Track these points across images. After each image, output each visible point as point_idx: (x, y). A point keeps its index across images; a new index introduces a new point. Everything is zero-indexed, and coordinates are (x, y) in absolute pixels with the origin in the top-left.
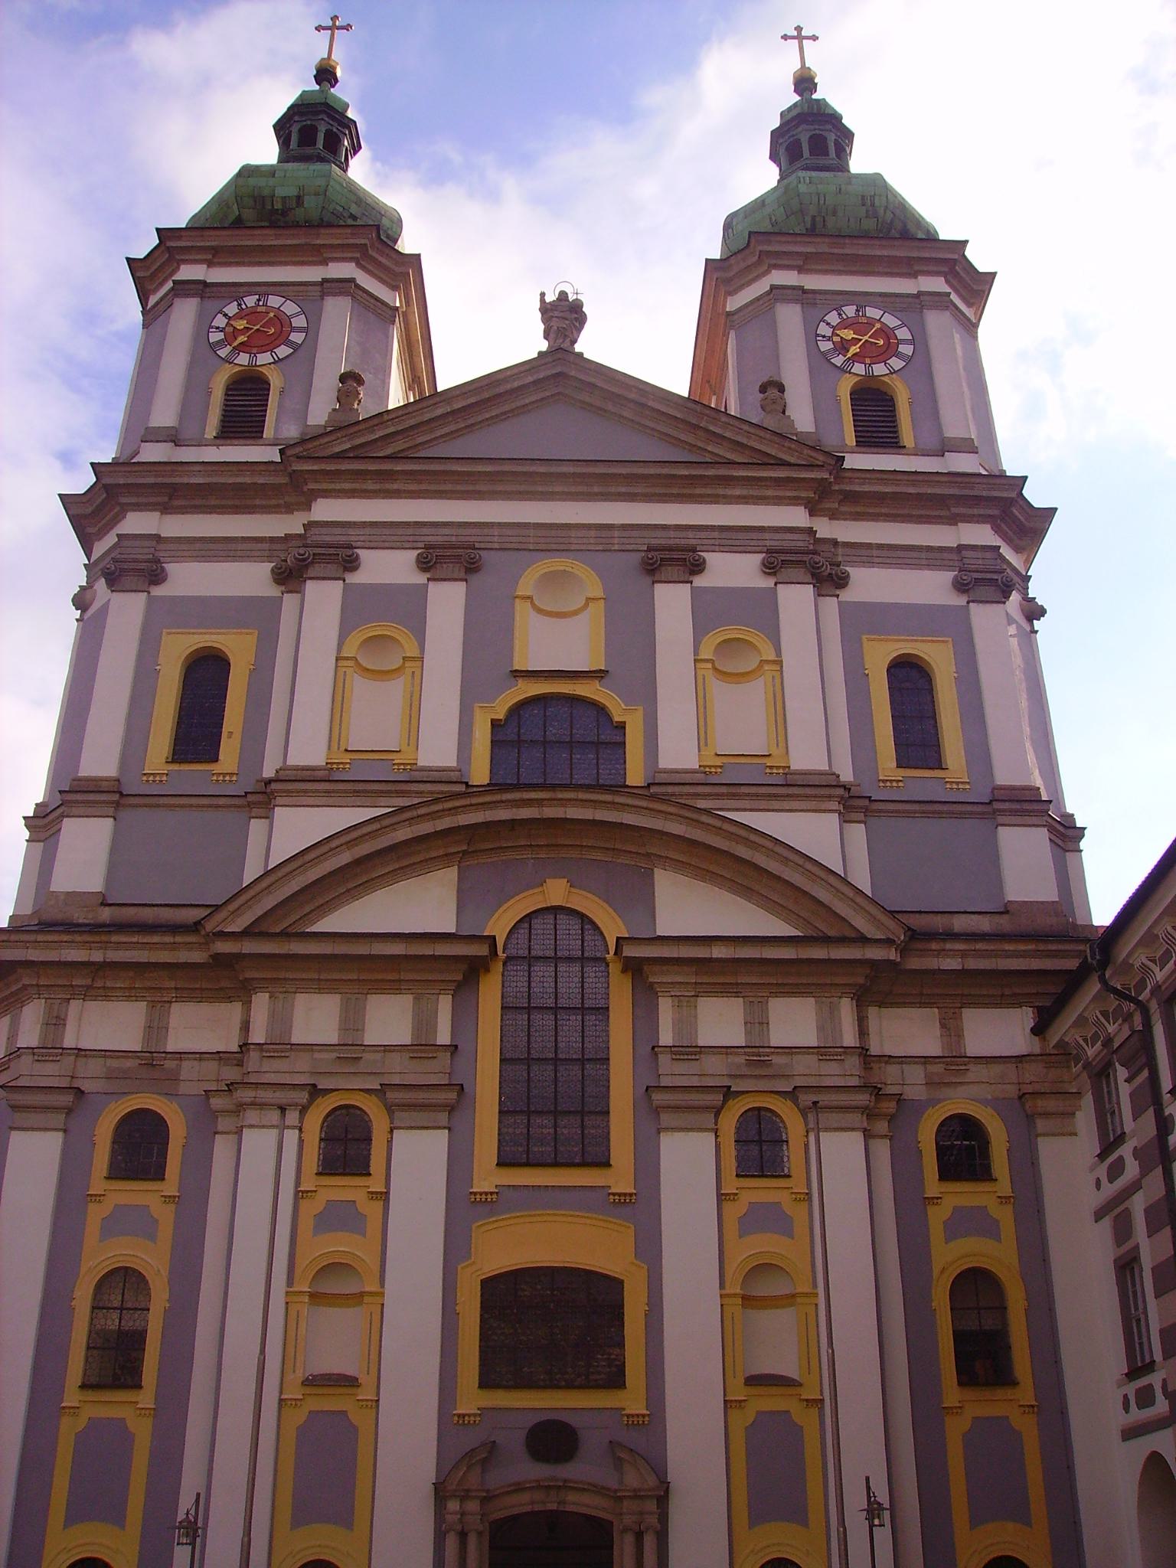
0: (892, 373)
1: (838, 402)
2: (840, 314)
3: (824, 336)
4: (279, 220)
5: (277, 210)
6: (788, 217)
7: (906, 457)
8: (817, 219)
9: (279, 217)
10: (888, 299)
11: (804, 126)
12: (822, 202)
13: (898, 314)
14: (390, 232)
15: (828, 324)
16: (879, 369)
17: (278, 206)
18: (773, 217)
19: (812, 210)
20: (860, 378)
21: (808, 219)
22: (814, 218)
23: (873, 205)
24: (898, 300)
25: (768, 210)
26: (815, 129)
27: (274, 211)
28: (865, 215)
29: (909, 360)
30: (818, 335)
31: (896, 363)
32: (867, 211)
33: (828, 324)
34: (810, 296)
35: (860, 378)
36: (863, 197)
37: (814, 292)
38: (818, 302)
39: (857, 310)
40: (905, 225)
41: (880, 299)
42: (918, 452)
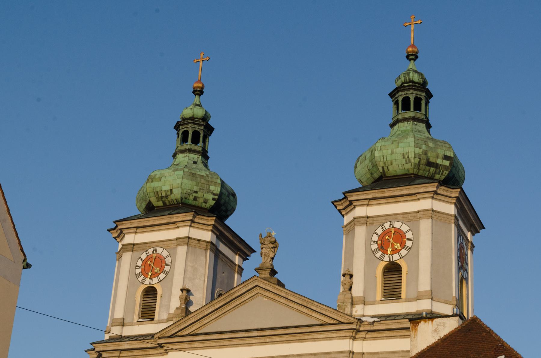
0: (401, 258)
1: (376, 277)
2: (383, 228)
3: (374, 242)
4: (165, 200)
5: (164, 196)
6: (373, 167)
7: (402, 303)
8: (385, 168)
9: (165, 199)
10: (405, 216)
11: (400, 93)
12: (385, 160)
13: (409, 224)
14: (214, 192)
15: (377, 234)
16: (396, 257)
17: (164, 195)
19: (382, 164)
20: (388, 262)
22: (383, 167)
23: (408, 157)
24: (409, 215)
26: (405, 94)
27: (162, 197)
28: (405, 163)
29: (409, 249)
30: (371, 241)
31: (404, 252)
32: (406, 161)
33: (377, 234)
34: (371, 219)
35: (388, 262)
36: (403, 154)
37: (373, 217)
38: (374, 222)
39: (391, 225)
40: (428, 160)
41: (401, 216)
42: (409, 300)
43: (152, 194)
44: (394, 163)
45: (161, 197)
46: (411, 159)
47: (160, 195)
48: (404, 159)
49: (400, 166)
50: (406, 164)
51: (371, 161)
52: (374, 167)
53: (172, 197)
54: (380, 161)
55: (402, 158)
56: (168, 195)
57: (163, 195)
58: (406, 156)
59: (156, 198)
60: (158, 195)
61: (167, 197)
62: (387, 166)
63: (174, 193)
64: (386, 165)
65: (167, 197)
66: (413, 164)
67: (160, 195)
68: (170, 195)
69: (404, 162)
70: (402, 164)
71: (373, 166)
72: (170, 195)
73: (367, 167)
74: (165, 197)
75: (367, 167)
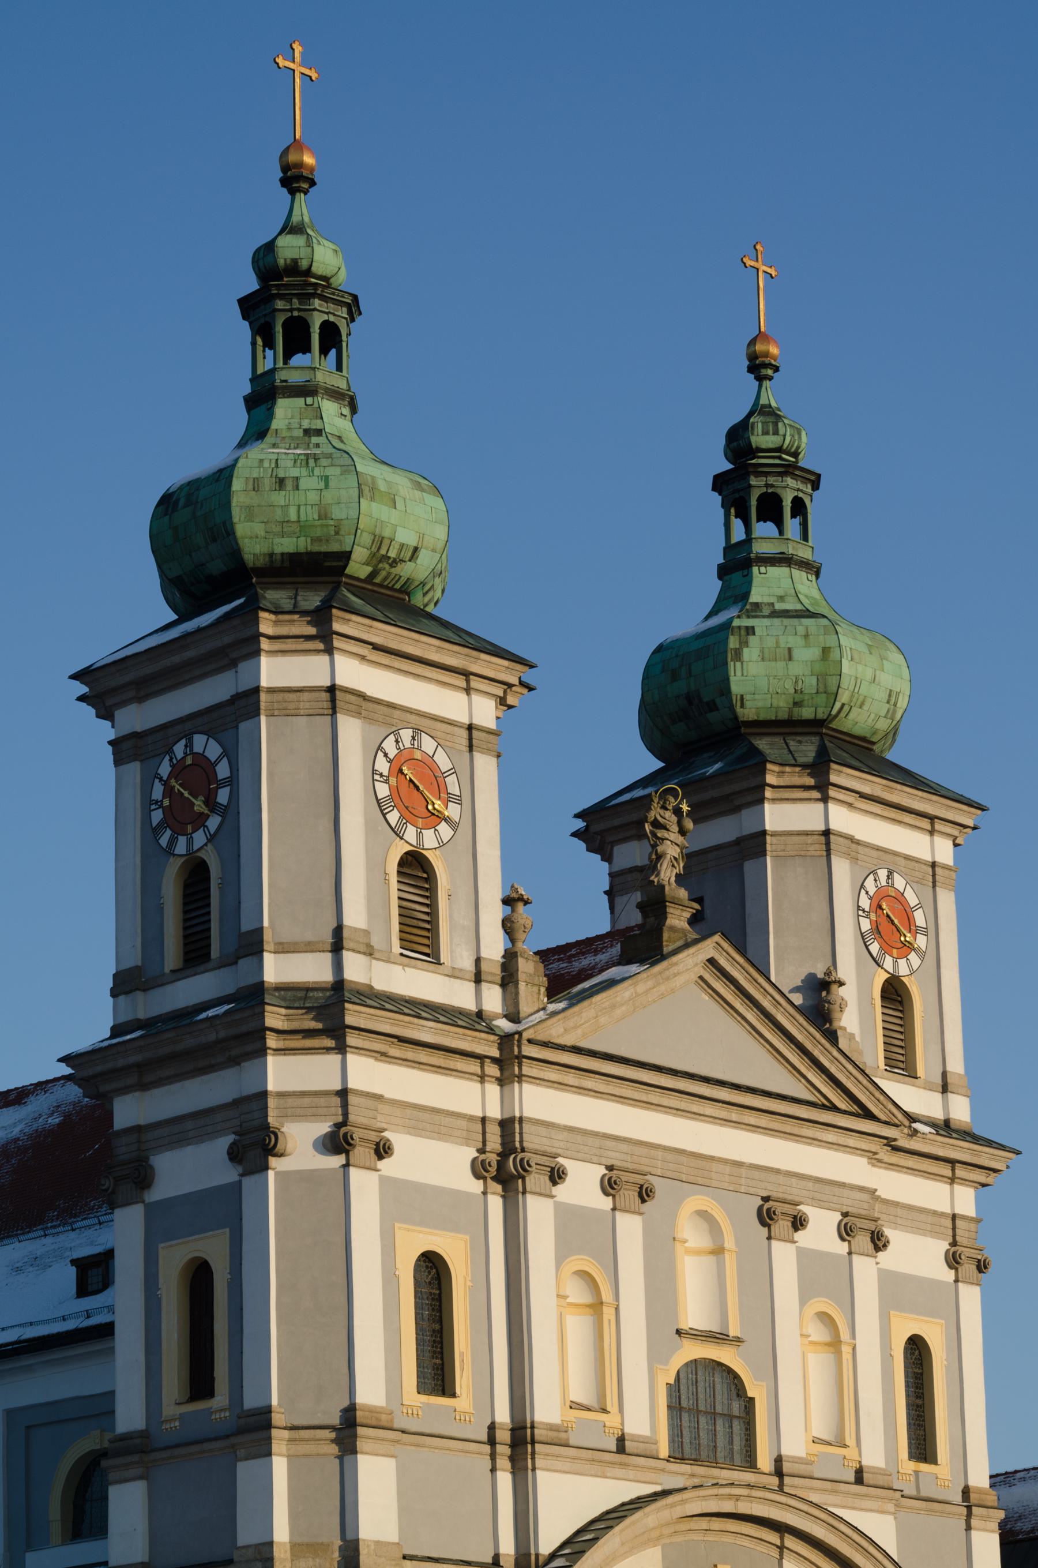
5: (389, 558)
6: (817, 693)
8: (846, 708)
17: (392, 554)
18: (800, 682)
21: (838, 705)
22: (843, 705)
23: (895, 705)
25: (796, 669)
32: (888, 711)
36: (890, 695)
43: (365, 539)
44: (865, 708)
45: (383, 555)
46: (898, 709)
47: (383, 552)
48: (888, 705)
49: (873, 716)
50: (885, 717)
51: (821, 678)
52: (825, 695)
53: (406, 570)
54: (848, 689)
55: (886, 701)
56: (400, 560)
57: (389, 555)
58: (892, 702)
59: (369, 552)
60: (379, 548)
61: (394, 563)
62: (851, 707)
63: (419, 561)
64: (852, 704)
65: (394, 563)
66: (895, 723)
67: (383, 552)
68: (405, 562)
69: (883, 713)
70: (876, 715)
71: (821, 690)
72: (405, 562)
73: (796, 682)
74: (390, 561)
75: (796, 682)
